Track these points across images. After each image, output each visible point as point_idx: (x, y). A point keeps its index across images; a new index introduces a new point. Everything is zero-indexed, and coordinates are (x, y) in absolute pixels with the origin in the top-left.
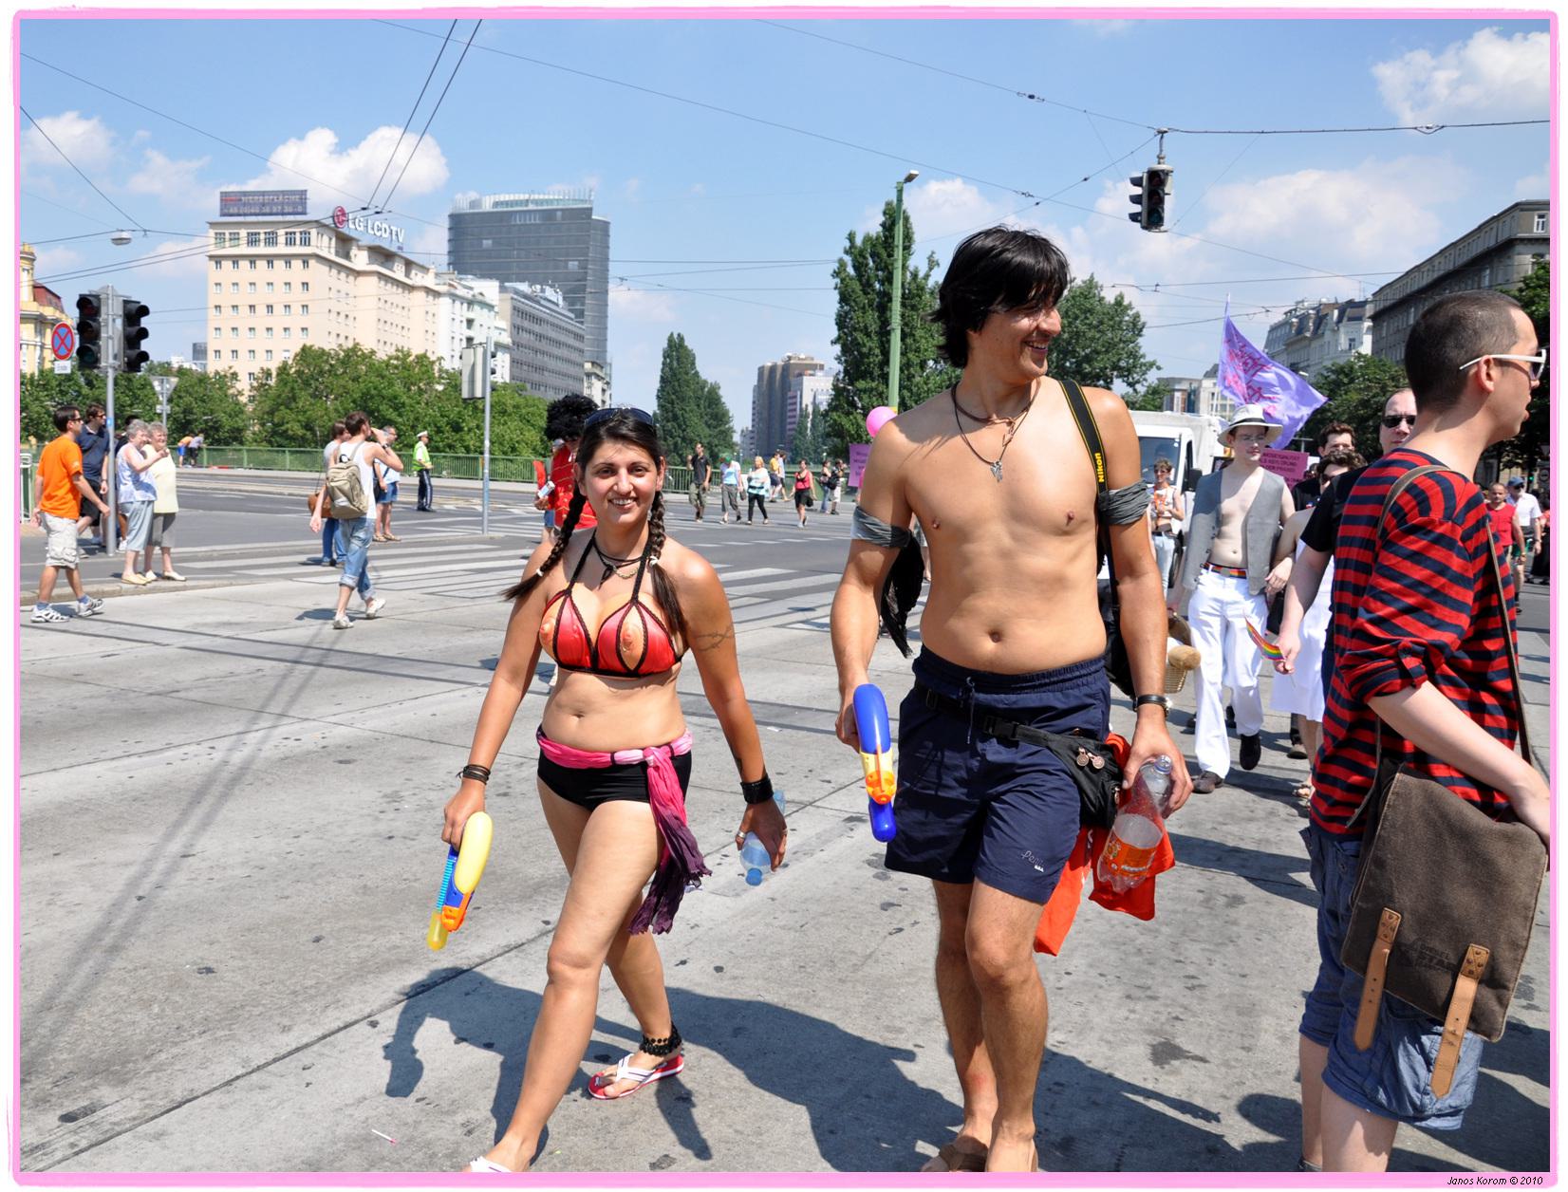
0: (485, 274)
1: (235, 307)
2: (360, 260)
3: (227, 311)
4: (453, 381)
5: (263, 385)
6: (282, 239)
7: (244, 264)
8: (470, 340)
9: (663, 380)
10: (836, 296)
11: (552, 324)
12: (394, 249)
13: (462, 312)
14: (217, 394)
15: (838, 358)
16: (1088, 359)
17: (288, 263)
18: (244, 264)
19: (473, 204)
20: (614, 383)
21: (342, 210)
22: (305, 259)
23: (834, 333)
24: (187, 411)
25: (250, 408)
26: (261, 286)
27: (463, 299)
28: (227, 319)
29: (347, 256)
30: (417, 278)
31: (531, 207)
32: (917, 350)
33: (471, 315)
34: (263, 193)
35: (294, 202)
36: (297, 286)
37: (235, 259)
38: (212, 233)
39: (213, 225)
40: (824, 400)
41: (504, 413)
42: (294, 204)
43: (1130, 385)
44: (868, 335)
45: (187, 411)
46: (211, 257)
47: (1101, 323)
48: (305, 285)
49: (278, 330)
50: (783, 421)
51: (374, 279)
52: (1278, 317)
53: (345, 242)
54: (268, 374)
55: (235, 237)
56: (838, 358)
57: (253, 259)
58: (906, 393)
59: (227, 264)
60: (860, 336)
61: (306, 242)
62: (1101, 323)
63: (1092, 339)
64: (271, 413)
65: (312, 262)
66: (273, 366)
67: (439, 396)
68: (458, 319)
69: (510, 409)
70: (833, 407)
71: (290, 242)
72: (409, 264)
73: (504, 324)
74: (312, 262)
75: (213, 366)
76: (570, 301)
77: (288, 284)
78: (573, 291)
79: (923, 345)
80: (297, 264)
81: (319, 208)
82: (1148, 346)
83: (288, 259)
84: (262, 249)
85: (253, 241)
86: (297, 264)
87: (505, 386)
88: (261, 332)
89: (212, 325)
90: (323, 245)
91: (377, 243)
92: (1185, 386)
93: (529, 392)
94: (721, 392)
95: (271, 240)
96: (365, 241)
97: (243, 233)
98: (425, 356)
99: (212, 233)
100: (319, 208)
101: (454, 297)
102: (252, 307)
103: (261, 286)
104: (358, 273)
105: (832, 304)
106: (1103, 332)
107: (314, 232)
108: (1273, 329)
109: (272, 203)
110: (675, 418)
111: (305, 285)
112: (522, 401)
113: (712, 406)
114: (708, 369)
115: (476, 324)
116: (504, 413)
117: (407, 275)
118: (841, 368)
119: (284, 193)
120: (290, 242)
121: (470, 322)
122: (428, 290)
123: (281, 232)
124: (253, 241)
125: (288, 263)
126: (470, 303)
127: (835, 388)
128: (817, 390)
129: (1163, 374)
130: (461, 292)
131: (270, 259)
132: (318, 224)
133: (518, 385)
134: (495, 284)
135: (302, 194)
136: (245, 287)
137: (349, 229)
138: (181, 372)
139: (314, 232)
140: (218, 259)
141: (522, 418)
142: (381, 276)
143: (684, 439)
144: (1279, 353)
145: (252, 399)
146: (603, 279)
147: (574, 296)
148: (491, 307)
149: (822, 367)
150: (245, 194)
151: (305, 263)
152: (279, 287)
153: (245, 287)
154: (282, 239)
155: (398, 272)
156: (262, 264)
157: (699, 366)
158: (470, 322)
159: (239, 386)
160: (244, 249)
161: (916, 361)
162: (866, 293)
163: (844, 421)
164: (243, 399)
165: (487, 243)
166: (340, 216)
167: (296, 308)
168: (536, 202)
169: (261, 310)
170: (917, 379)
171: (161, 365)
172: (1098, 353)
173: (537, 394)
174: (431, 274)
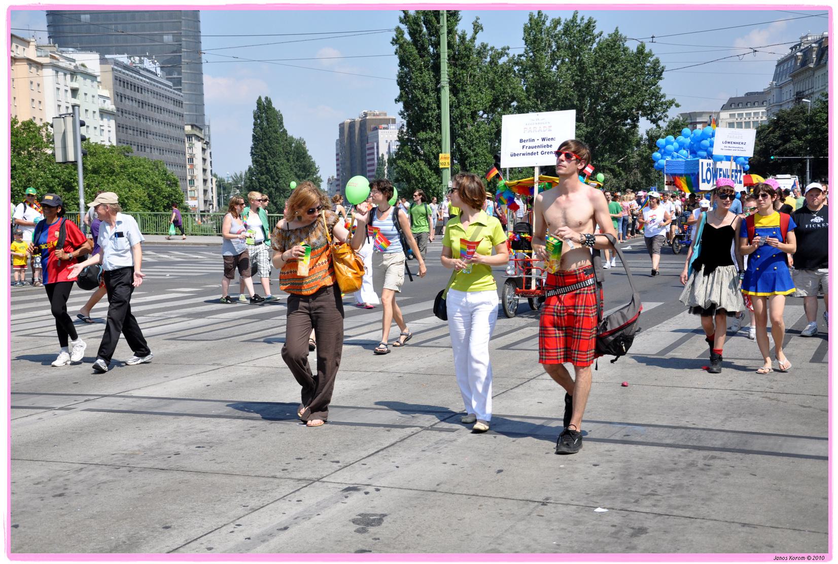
9: (255, 138)
10: (398, 61)
11: (153, 92)
15: (401, 114)
16: (616, 102)
20: (212, 143)
23: (397, 91)
27: (66, 71)
32: (469, 103)
33: (75, 85)
40: (394, 148)
41: (112, 172)
43: (653, 121)
44: (426, 91)
47: (626, 69)
52: (786, 51)
56: (401, 114)
58: (460, 140)
60: (418, 93)
62: (626, 69)
63: (618, 85)
68: (62, 88)
69: (117, 169)
70: (400, 155)
78: (168, 62)
79: (473, 98)
82: (667, 87)
87: (112, 149)
92: (705, 119)
93: (135, 153)
94: (308, 146)
101: (57, 68)
105: (393, 67)
106: (628, 78)
108: (780, 63)
110: (268, 171)
112: (128, 162)
114: (293, 128)
116: (112, 172)
121: (74, 92)
126: (73, 74)
127: (400, 139)
128: (387, 141)
129: (686, 109)
130: (63, 63)
133: (124, 148)
134: (96, 56)
141: (130, 177)
143: (277, 189)
144: (786, 84)
146: (197, 52)
148: (93, 77)
157: (287, 125)
158: (74, 92)
161: (469, 112)
162: (422, 56)
163: (411, 169)
170: (470, 128)
172: (624, 96)
173: (143, 155)
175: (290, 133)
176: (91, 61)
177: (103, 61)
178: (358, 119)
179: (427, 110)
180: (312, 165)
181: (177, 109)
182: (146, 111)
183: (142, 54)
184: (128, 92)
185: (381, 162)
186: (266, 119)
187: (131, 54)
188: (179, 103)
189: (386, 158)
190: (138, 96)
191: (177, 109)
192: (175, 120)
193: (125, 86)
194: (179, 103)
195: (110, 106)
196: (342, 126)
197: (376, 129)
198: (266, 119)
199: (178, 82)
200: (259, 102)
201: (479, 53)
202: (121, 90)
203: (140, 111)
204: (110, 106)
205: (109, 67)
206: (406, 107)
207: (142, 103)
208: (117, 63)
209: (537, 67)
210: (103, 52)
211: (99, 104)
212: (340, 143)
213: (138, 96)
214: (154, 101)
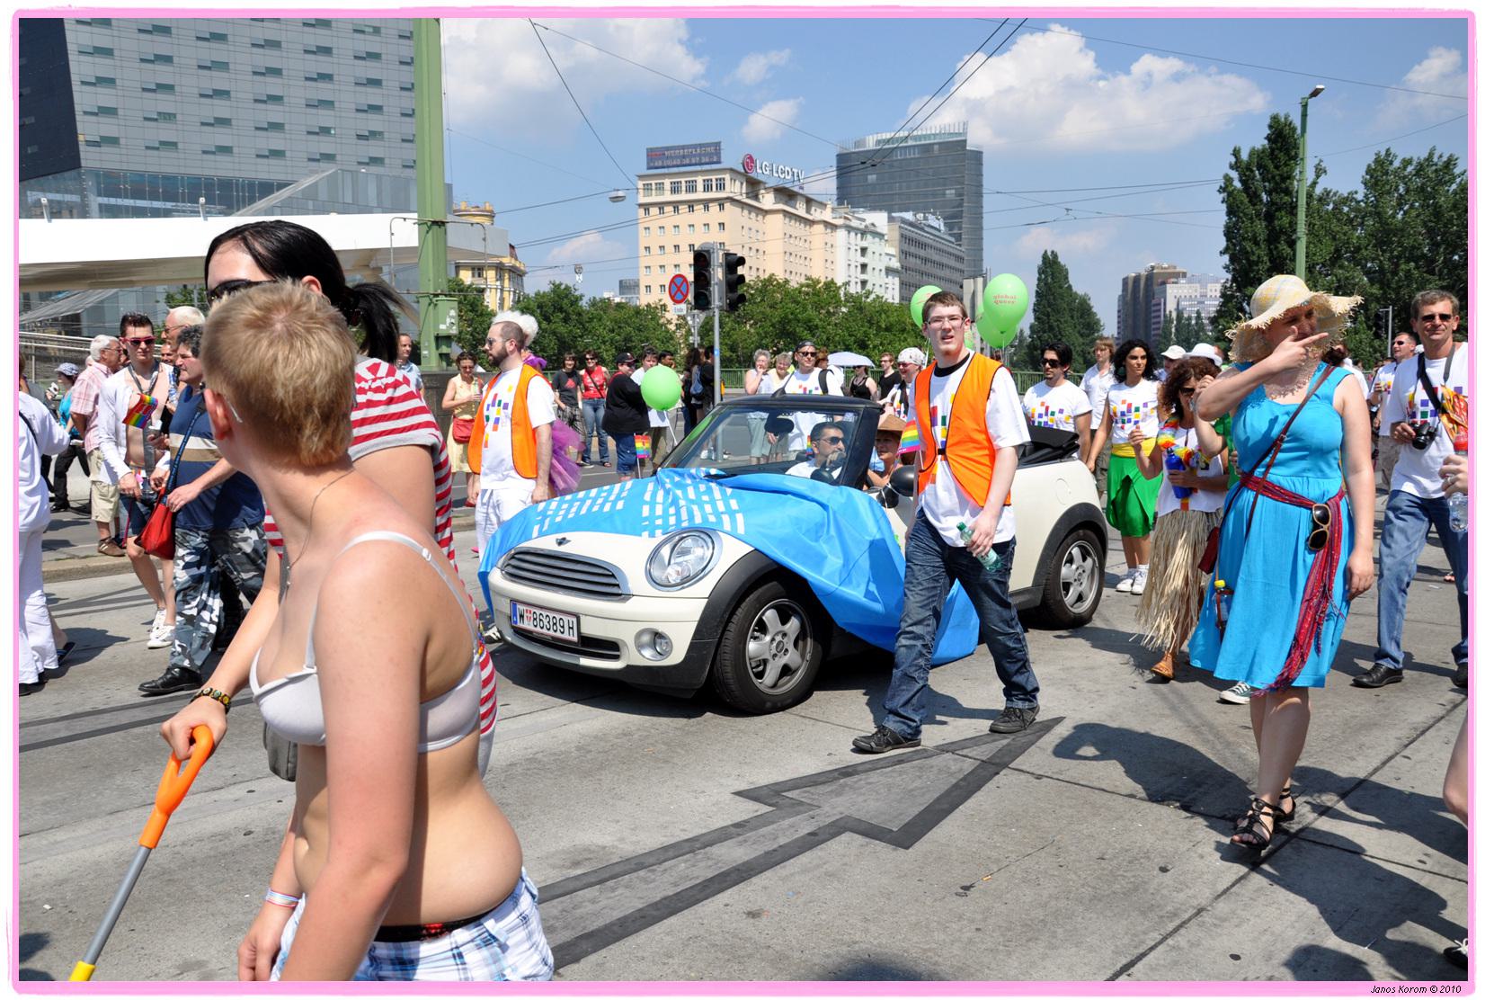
0: (873, 208)
1: (662, 248)
2: (768, 201)
3: (655, 250)
4: (857, 304)
6: (700, 186)
8: (864, 266)
12: (796, 189)
13: (857, 241)
14: (652, 324)
17: (707, 208)
18: (669, 209)
19: (857, 144)
21: (750, 158)
22: (721, 203)
24: (628, 339)
27: (856, 230)
28: (655, 259)
29: (756, 198)
30: (817, 214)
31: (910, 143)
33: (864, 244)
34: (683, 147)
36: (715, 227)
37: (661, 206)
38: (640, 184)
39: (641, 177)
42: (710, 155)
45: (628, 339)
46: (641, 205)
48: (722, 225)
50: (1147, 327)
51: (781, 216)
53: (754, 186)
55: (660, 187)
57: (676, 205)
59: (654, 211)
61: (721, 187)
65: (727, 205)
67: (846, 317)
71: (707, 188)
72: (809, 201)
73: (893, 251)
74: (727, 205)
75: (644, 299)
76: (949, 226)
77: (707, 225)
80: (714, 207)
81: (732, 158)
83: (706, 204)
85: (675, 190)
86: (714, 207)
89: (643, 262)
90: (736, 189)
91: (780, 184)
94: (1092, 303)
95: (691, 188)
96: (772, 183)
97: (667, 183)
98: (832, 281)
99: (640, 184)
100: (732, 158)
101: (849, 229)
102: (677, 247)
103: (684, 229)
104: (767, 212)
107: (727, 177)
109: (691, 155)
110: (1051, 328)
111: (722, 225)
113: (1084, 314)
114: (1079, 284)
115: (869, 252)
117: (808, 211)
118: (1229, 276)
119: (701, 146)
120: (707, 188)
121: (864, 250)
122: (826, 224)
123: (700, 179)
124: (675, 190)
125: (707, 208)
126: (864, 233)
130: (855, 223)
131: (691, 205)
132: (732, 170)
135: (718, 145)
136: (670, 230)
137: (757, 174)
138: (619, 305)
139: (727, 182)
142: (786, 213)
147: (953, 220)
148: (881, 236)
149: (1184, 275)
150: (668, 149)
151: (721, 206)
152: (700, 228)
153: (670, 230)
154: (700, 186)
155: (800, 209)
156: (683, 208)
157: (1072, 280)
158: (864, 250)
159: (668, 316)
160: (668, 197)
165: (872, 178)
166: (749, 161)
168: (916, 138)
171: (602, 300)
174: (829, 209)
175: (1074, 289)
176: (879, 219)
177: (891, 219)
178: (1144, 273)
179: (1256, 264)
180: (1098, 322)
181: (958, 265)
182: (928, 268)
183: (925, 210)
184: (913, 249)
185: (1168, 321)
186: (1051, 274)
187: (916, 210)
188: (960, 259)
189: (1174, 315)
190: (922, 253)
191: (958, 265)
192: (956, 276)
193: (911, 243)
194: (960, 259)
195: (895, 264)
196: (1125, 281)
197: (1164, 283)
198: (1051, 274)
199: (958, 237)
200: (1045, 256)
201: (1320, 199)
202: (906, 247)
203: (923, 268)
204: (895, 264)
205: (896, 226)
206: (1232, 260)
207: (925, 260)
208: (904, 221)
209: (1378, 214)
210: (890, 210)
211: (885, 262)
212: (1123, 298)
213: (922, 253)
214: (936, 257)
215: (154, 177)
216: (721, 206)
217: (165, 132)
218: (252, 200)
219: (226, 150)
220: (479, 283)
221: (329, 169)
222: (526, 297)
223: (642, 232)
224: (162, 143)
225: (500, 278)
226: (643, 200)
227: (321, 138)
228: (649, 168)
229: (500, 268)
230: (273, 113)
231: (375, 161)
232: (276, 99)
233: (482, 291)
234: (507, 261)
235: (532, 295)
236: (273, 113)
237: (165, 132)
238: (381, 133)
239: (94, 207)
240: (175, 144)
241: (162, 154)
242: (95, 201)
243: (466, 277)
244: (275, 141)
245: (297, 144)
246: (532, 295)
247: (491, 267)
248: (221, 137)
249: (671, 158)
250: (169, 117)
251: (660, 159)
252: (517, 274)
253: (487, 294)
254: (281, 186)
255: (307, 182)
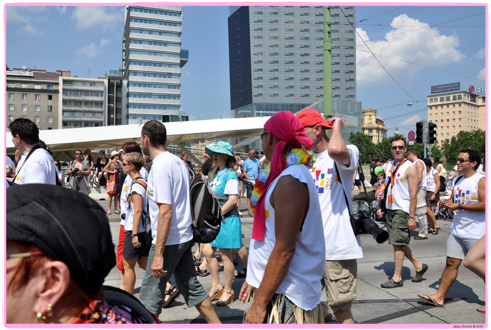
5: (446, 144)
6: (451, 98)
7: (439, 107)
17: (454, 106)
18: (439, 107)
22: (460, 104)
25: (442, 151)
26: (445, 114)
34: (445, 85)
35: (455, 87)
37: (436, 106)
38: (429, 99)
39: (429, 96)
42: (456, 87)
46: (429, 106)
49: (451, 127)
54: (448, 141)
55: (436, 99)
57: (442, 105)
59: (434, 108)
64: (450, 153)
66: (450, 138)
71: (454, 99)
80: (457, 105)
84: (445, 102)
85: (442, 100)
86: (457, 105)
88: (445, 128)
95: (448, 99)
97: (439, 98)
99: (429, 99)
102: (442, 120)
103: (445, 114)
109: (448, 88)
111: (460, 112)
119: (452, 84)
125: (454, 106)
140: (431, 107)
145: (442, 149)
150: (439, 86)
151: (460, 105)
152: (451, 113)
154: (451, 98)
156: (445, 107)
159: (438, 145)
160: (439, 103)
164: (440, 149)
167: (457, 120)
169: (445, 120)
215: (272, 104)
216: (460, 105)
217: (275, 91)
218: (299, 110)
219: (292, 95)
220: (371, 134)
221: (321, 99)
222: (386, 139)
223: (429, 116)
224: (274, 94)
225: (378, 132)
226: (429, 104)
227: (321, 90)
228: (432, 93)
229: (378, 129)
230: (306, 83)
231: (337, 96)
232: (307, 79)
233: (372, 137)
234: (380, 126)
235: (388, 138)
236: (306, 83)
237: (275, 91)
238: (339, 87)
239: (255, 114)
240: (277, 95)
241: (274, 97)
242: (256, 112)
243: (366, 132)
244: (306, 92)
245: (313, 92)
246: (388, 138)
247: (374, 129)
248: (291, 91)
249: (440, 89)
250: (276, 87)
251: (436, 90)
252: (384, 131)
253: (374, 137)
254: (308, 105)
255: (315, 104)
